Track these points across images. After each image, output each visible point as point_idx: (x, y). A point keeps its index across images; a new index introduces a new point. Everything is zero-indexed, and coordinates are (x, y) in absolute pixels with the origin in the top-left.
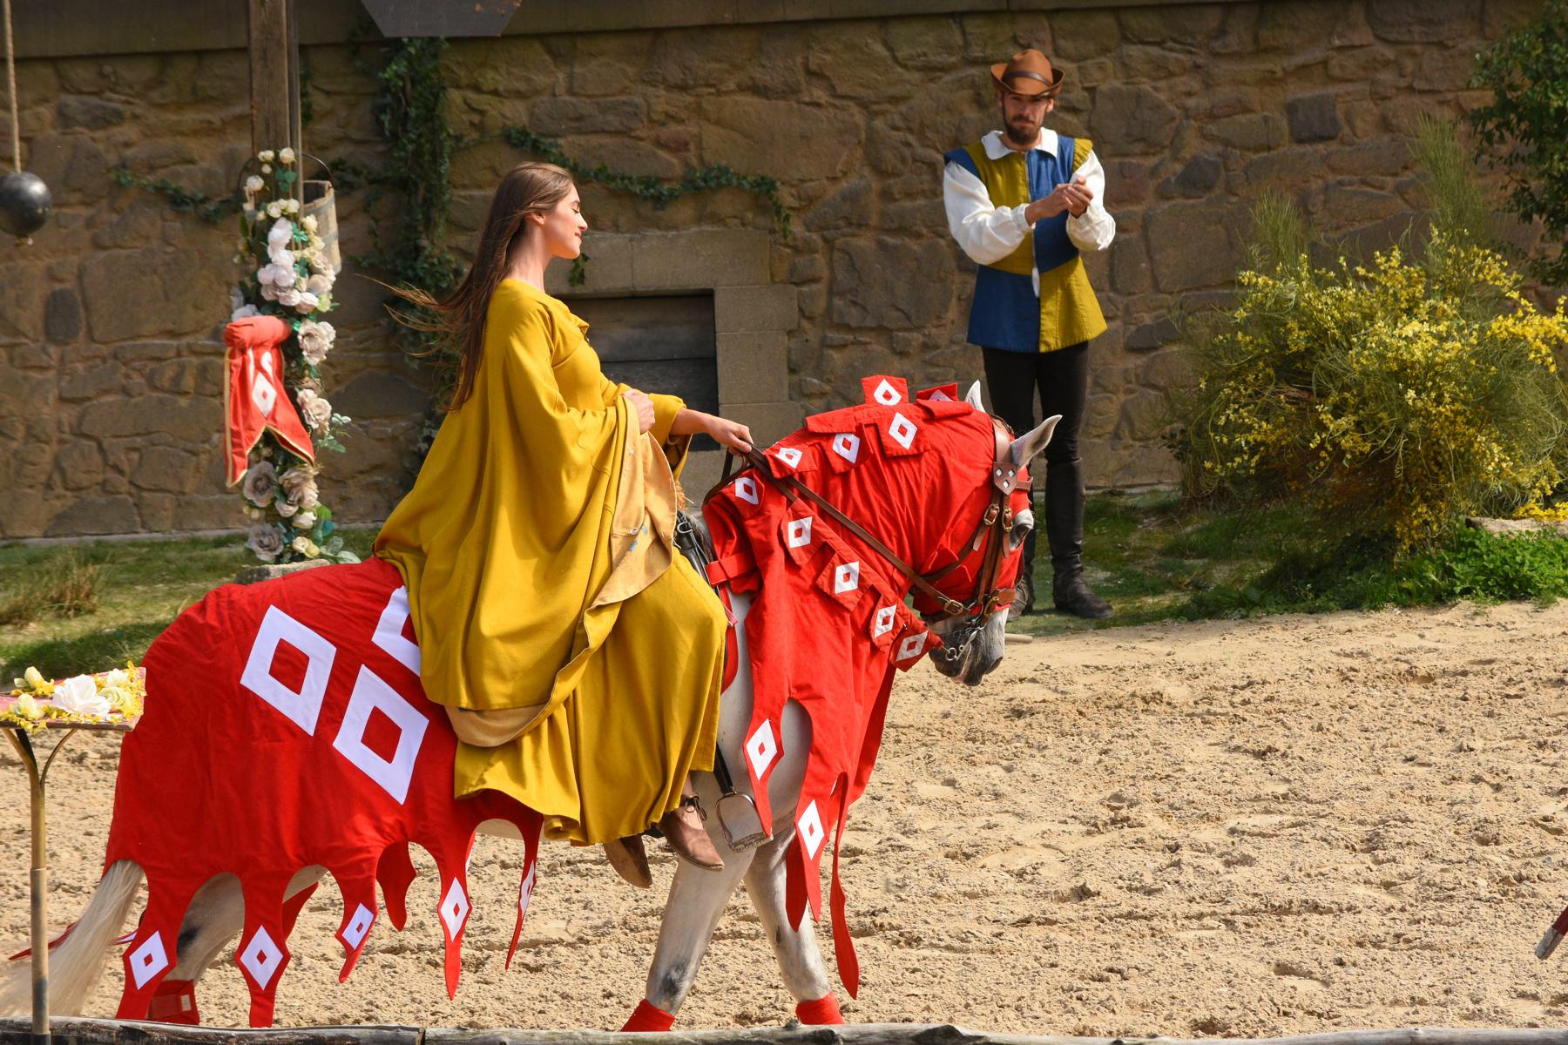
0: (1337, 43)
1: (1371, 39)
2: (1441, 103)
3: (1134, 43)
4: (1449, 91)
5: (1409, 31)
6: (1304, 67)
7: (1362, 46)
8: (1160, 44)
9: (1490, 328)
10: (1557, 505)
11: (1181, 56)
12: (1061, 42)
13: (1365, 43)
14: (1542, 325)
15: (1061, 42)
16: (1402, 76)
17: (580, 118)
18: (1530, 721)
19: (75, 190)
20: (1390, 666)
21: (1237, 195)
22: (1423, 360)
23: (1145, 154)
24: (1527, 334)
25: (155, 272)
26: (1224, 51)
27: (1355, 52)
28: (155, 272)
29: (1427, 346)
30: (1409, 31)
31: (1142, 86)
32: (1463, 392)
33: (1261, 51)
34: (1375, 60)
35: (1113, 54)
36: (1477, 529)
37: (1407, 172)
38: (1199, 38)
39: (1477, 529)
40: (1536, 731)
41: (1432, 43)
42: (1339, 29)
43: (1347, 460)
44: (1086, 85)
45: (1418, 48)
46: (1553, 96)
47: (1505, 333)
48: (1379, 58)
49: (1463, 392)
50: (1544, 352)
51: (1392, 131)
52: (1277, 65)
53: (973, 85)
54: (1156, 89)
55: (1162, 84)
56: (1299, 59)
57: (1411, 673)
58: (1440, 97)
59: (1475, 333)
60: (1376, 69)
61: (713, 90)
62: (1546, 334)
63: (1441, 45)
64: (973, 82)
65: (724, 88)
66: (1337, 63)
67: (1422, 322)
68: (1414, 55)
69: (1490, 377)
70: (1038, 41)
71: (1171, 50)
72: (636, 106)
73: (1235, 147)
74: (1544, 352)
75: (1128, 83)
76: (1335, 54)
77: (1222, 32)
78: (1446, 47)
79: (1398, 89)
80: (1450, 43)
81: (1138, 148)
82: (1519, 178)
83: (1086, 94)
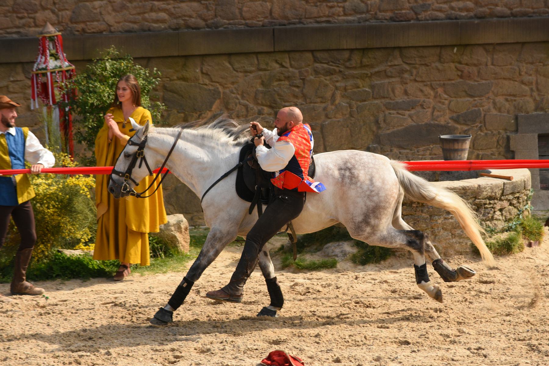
0: (389, 64)
1: (402, 63)
2: (425, 85)
3: (318, 63)
4: (428, 81)
5: (415, 60)
6: (379, 72)
7: (398, 65)
8: (327, 63)
9: (67, 182)
10: (90, 245)
11: (335, 68)
12: (293, 63)
13: (22, 79)
14: (85, 181)
15: (293, 63)
16: (412, 76)
17: (496, 74)
18: (80, 322)
19: (319, 97)
20: (30, 302)
21: (353, 117)
22: (42, 193)
23: (321, 102)
24: (80, 184)
25: (348, 127)
26: (350, 66)
27: (395, 67)
28: (348, 127)
29: (44, 188)
30: (415, 60)
31: (321, 78)
32: (56, 204)
33: (362, 66)
34: (403, 70)
35: (311, 67)
36: (61, 253)
37: (413, 110)
38: (341, 61)
39: (61, 253)
40: (82, 325)
41: (423, 64)
42: (390, 59)
43: (16, 229)
44: (301, 78)
45: (417, 66)
46: (89, 99)
47: (72, 184)
48: (404, 69)
49: (56, 204)
50: (86, 190)
51: (408, 95)
52: (368, 71)
53: (260, 77)
54: (326, 80)
55: (328, 78)
56: (376, 69)
57: (37, 305)
58: (425, 84)
59: (61, 184)
60: (403, 73)
61: (542, 64)
62: (87, 184)
63: (426, 65)
64: (261, 77)
65: (172, 78)
66: (12, 87)
67: (42, 179)
68: (415, 68)
69: (67, 199)
70: (285, 62)
71: (332, 65)
72: (515, 69)
73: (353, 100)
74: (86, 190)
75: (316, 77)
76: (388, 67)
77: (349, 59)
78: (428, 66)
79: (411, 80)
80: (429, 64)
81: (319, 100)
82: (77, 128)
83: (301, 81)
